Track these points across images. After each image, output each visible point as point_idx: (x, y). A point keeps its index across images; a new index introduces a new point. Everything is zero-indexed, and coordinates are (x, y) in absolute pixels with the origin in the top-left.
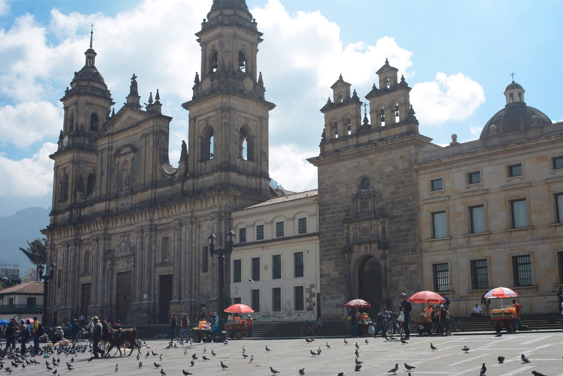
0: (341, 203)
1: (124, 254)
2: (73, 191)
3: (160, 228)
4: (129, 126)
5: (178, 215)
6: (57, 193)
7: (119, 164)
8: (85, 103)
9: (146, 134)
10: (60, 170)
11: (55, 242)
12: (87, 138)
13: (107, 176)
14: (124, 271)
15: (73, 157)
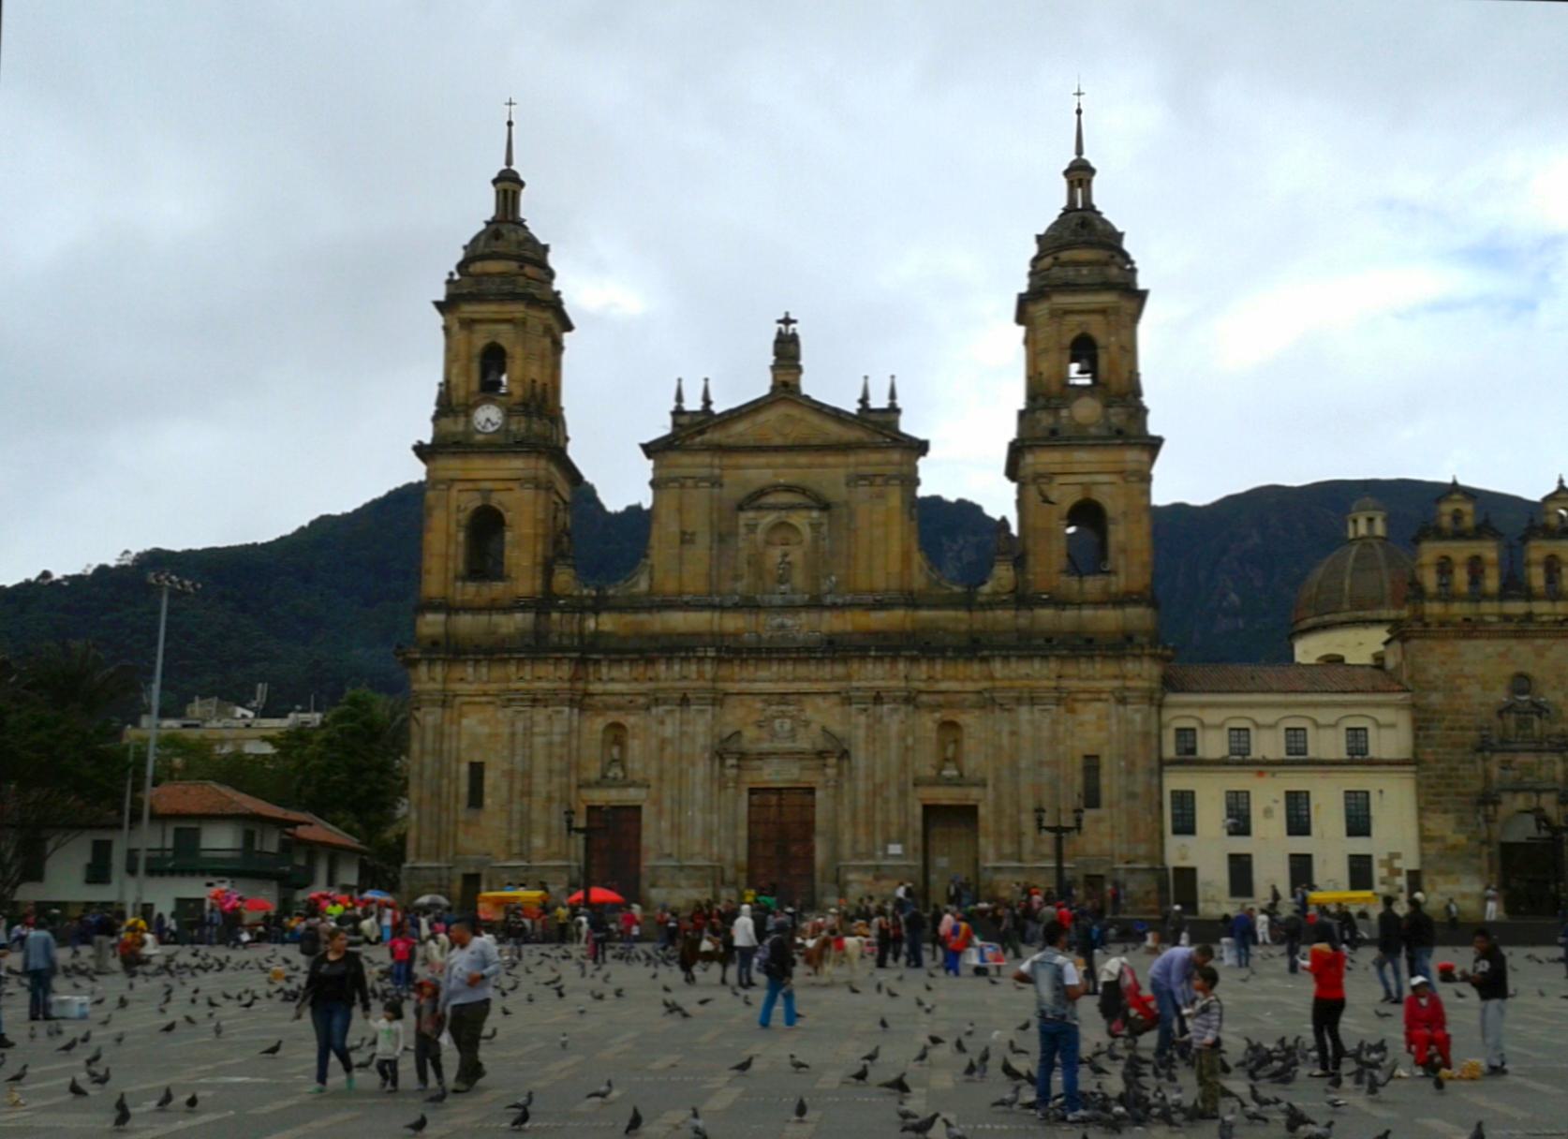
0: (1470, 714)
1: (788, 745)
2: (539, 559)
3: (924, 698)
4: (789, 442)
5: (1010, 679)
6: (452, 550)
7: (756, 526)
9: (875, 475)
10: (460, 491)
11: (458, 687)
13: (711, 549)
14: (781, 785)
15: (536, 469)
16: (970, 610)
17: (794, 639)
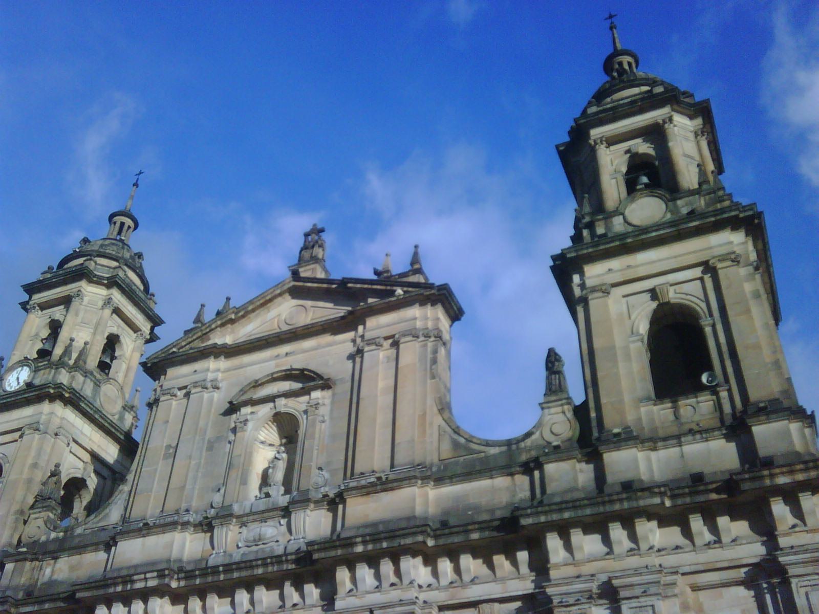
2: (16, 507)
7: (247, 420)
8: (101, 303)
12: (91, 380)
16: (512, 474)
17: (272, 550)
